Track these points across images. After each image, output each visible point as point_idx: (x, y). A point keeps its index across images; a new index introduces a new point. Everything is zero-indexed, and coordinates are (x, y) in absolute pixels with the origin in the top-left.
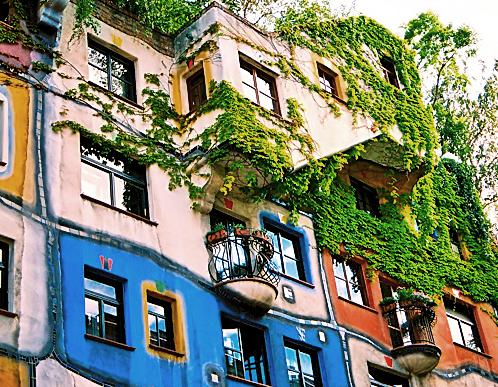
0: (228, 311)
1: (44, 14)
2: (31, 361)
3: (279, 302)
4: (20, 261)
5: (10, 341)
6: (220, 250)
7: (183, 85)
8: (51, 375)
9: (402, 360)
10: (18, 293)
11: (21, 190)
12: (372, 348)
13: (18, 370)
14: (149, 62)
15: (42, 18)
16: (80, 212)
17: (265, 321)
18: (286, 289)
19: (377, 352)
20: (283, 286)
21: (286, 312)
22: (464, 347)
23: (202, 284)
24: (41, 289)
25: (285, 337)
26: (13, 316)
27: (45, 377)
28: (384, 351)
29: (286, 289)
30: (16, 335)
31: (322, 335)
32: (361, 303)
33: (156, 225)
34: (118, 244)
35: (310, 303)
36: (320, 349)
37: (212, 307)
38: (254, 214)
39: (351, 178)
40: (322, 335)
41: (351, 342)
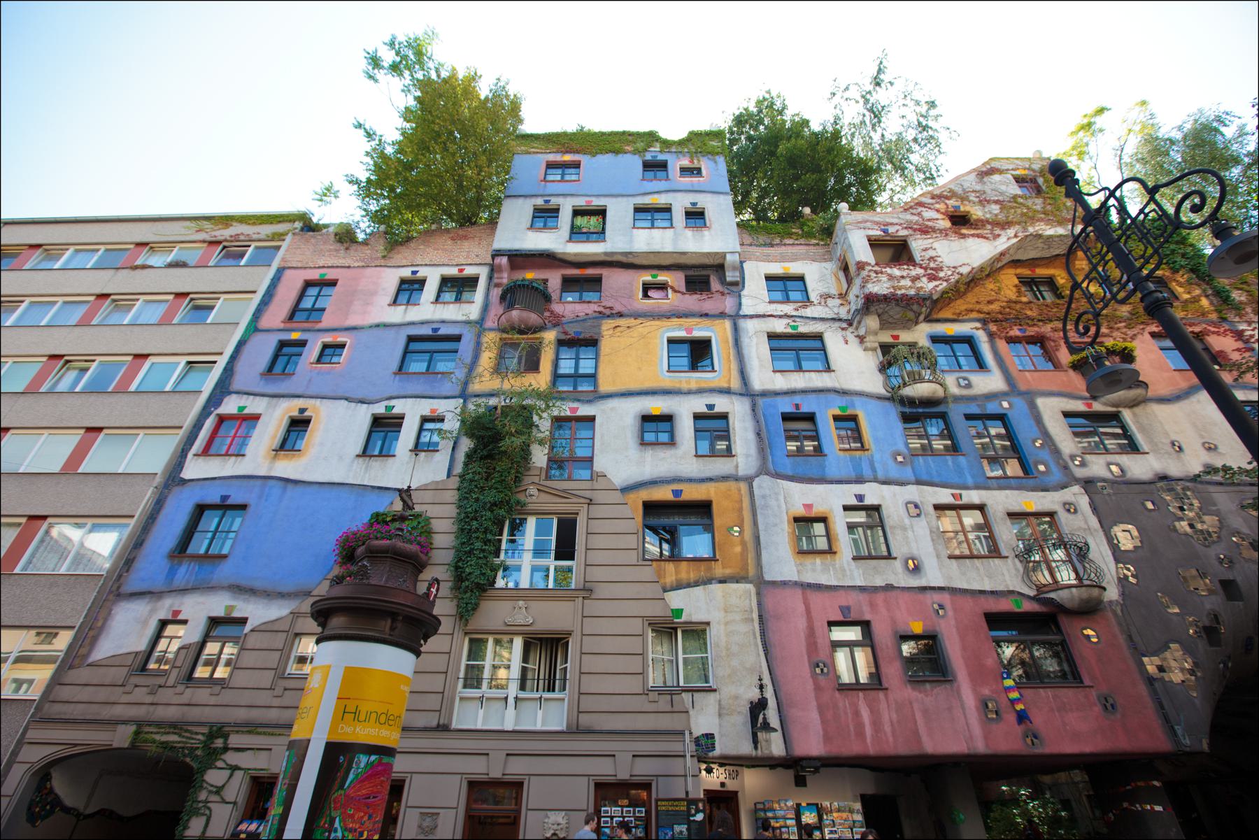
0: (907, 410)
1: (731, 276)
2: (749, 480)
3: (954, 390)
5: (732, 471)
6: (894, 370)
11: (729, 381)
12: (1065, 400)
23: (880, 398)
24: (751, 436)
27: (760, 487)
30: (737, 467)
31: (1005, 404)
34: (804, 392)
35: (991, 382)
37: (892, 413)
40: (1005, 404)
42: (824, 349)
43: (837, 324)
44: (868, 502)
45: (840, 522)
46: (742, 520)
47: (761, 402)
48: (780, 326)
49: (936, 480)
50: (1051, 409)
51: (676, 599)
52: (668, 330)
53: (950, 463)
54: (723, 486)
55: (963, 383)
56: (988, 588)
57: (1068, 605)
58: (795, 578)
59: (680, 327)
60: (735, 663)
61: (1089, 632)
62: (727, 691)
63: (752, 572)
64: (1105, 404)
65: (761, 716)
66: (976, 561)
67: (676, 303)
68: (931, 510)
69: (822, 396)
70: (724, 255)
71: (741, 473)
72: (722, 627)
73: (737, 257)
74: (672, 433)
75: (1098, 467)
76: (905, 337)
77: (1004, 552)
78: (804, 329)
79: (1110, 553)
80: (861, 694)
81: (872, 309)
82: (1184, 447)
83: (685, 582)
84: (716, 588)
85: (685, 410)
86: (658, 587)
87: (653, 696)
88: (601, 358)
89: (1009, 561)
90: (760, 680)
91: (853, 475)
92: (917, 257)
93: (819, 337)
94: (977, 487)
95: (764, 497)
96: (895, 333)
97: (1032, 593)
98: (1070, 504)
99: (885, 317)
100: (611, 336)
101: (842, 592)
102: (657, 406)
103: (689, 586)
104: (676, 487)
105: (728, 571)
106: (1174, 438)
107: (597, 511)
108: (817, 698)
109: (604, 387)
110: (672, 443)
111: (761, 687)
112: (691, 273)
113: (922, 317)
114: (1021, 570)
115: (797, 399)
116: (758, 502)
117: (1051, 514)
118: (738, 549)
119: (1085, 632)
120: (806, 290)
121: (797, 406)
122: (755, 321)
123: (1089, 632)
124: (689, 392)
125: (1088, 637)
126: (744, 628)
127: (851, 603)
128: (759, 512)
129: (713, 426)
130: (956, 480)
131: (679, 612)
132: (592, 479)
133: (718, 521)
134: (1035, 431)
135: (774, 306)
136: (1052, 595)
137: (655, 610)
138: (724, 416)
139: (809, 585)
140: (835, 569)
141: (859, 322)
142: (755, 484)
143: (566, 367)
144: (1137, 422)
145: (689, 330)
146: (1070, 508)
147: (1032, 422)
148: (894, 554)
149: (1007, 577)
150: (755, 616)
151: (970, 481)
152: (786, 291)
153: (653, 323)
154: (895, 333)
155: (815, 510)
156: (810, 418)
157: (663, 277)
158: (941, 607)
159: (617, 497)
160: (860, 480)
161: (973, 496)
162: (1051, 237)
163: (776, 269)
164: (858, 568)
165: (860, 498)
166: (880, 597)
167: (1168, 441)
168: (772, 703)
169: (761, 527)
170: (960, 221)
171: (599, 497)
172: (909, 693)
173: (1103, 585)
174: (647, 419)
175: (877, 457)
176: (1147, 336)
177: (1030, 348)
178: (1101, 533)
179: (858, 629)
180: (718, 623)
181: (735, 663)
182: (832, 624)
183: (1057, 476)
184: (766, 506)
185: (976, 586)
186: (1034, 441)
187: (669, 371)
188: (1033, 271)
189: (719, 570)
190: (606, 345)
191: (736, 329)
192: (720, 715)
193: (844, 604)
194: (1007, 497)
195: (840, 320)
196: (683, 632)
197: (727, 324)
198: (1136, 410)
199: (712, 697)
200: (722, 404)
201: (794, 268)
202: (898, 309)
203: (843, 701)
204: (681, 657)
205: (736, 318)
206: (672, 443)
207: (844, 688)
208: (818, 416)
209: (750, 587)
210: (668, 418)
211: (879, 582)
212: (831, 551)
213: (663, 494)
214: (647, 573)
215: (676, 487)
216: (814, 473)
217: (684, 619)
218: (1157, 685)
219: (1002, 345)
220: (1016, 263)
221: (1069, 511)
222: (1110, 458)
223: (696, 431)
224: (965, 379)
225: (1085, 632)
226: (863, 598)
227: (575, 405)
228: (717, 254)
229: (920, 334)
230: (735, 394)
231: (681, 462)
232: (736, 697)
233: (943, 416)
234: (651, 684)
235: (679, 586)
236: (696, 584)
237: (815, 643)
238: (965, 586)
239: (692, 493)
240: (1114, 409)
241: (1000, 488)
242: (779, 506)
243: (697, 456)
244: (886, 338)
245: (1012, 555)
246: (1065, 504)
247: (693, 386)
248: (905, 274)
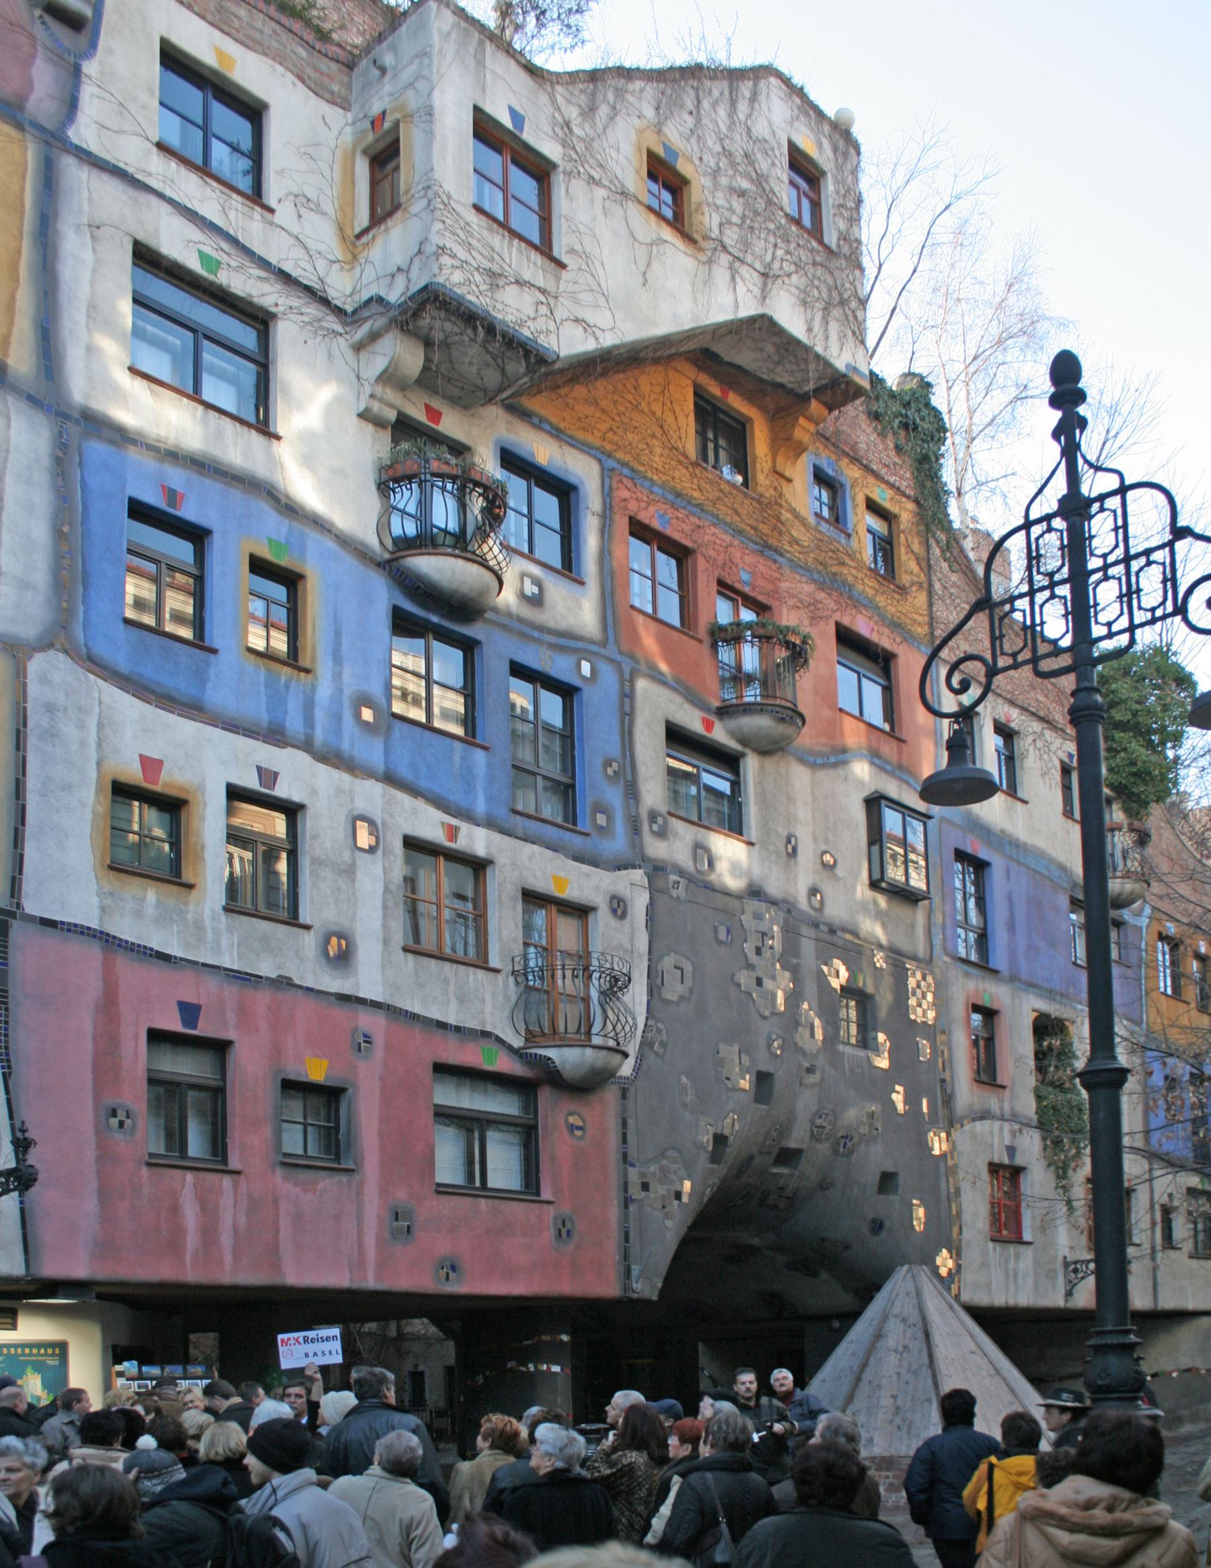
3: (508, 597)
37: (382, 596)
38: (484, 437)
56: (452, 1020)
66: (447, 965)
89: (500, 977)
114: (514, 999)
127: (202, 1001)
149: (488, 1008)
158: (368, 1039)
166: (263, 999)
178: (646, 963)
185: (435, 1013)
226: (231, 991)
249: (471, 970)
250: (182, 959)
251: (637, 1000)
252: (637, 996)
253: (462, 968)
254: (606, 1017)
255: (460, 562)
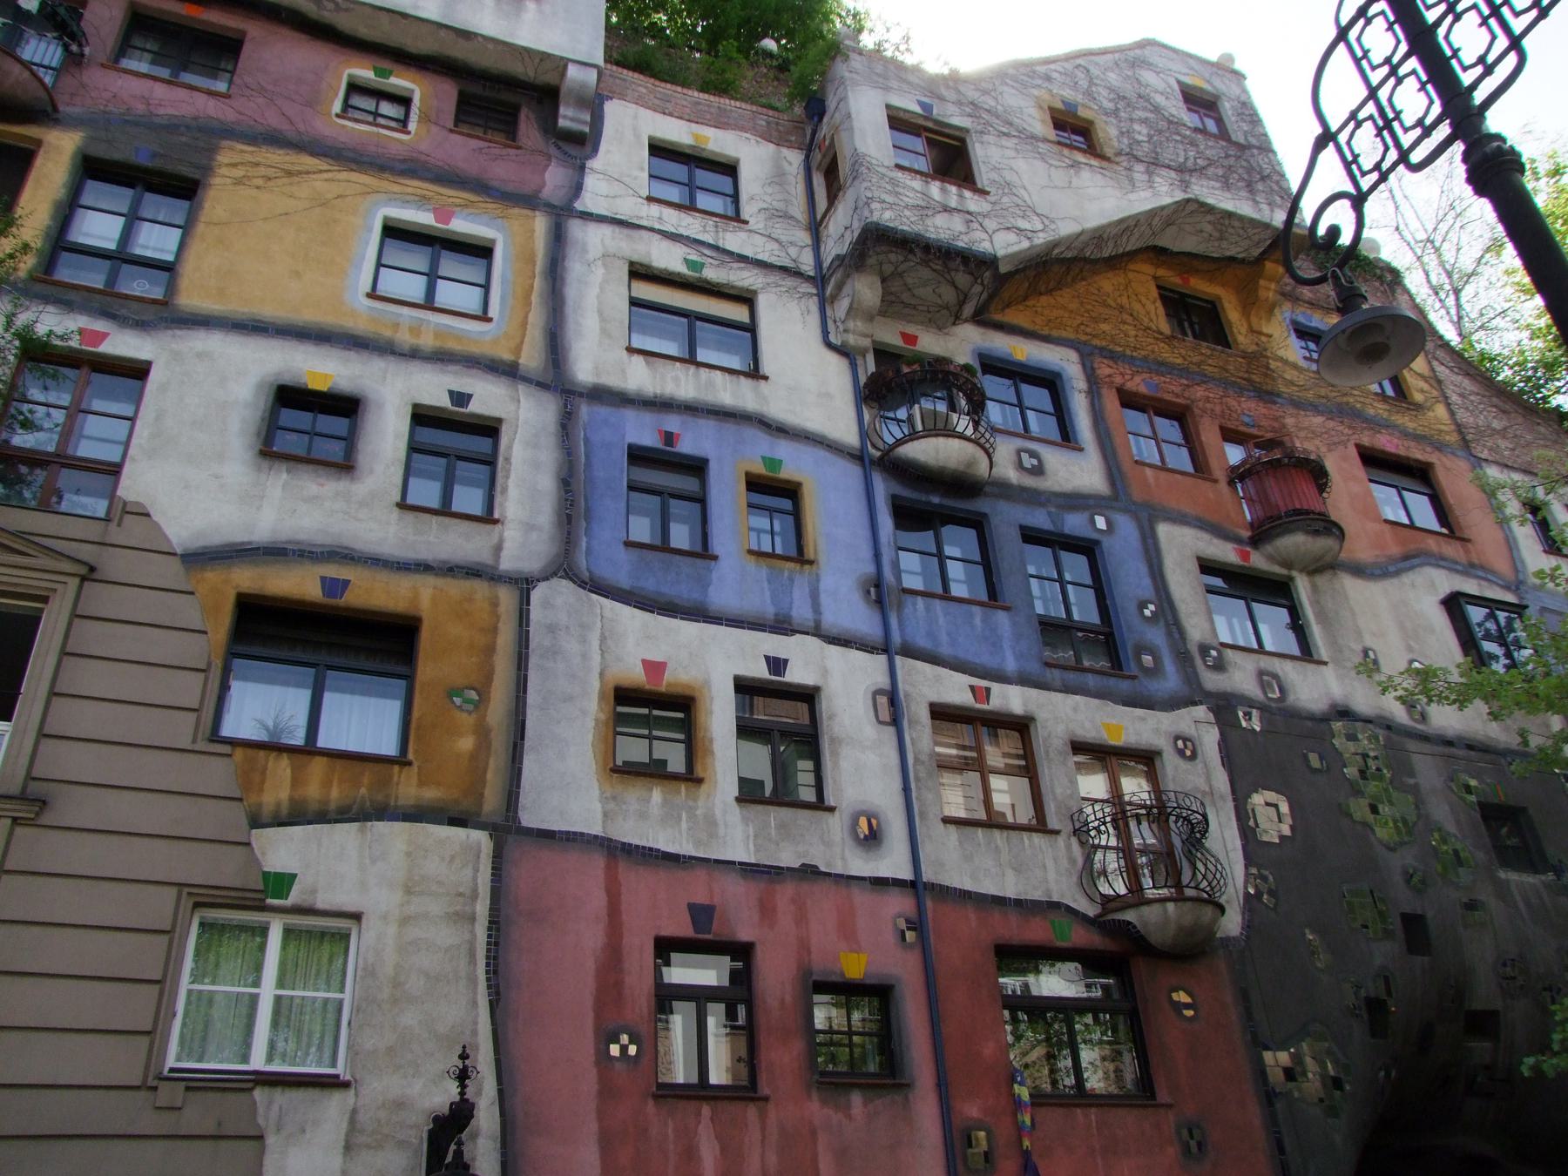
1: (569, 117)
2: (524, 585)
4: (510, 447)
7: (819, 181)
8: (559, 601)
9: (1269, 548)
10: (505, 490)
11: (518, 350)
12: (1206, 536)
13: (497, 597)
14: (763, 163)
15: (562, 123)
16: (623, 371)
17: (980, 505)
18: (1025, 456)
19: (1215, 541)
20: (1019, 452)
21: (1023, 489)
22: (1412, 526)
24: (547, 483)
25: (1022, 528)
26: (496, 522)
27: (547, 604)
28: (1237, 540)
29: (1025, 456)
30: (498, 548)
31: (1101, 522)
32: (1190, 468)
33: (766, 378)
34: (691, 409)
35: (1078, 471)
36: (1097, 542)
39: (1158, 287)
40: (1101, 522)
41: (1163, 530)
42: (751, 329)
43: (790, 282)
44: (796, 675)
45: (720, 717)
46: (489, 677)
47: (585, 410)
48: (669, 258)
49: (945, 650)
50: (1181, 545)
51: (282, 850)
52: (393, 199)
53: (978, 621)
54: (456, 588)
55: (1028, 462)
56: (1011, 892)
57: (1155, 938)
58: (596, 829)
59: (422, 201)
60: (410, 1018)
61: (1182, 997)
62: (378, 1087)
63: (492, 801)
64: (1271, 558)
65: (453, 1147)
66: (997, 833)
67: (424, 147)
68: (924, 715)
69: (730, 428)
70: (561, 64)
71: (507, 564)
72: (392, 930)
73: (592, 76)
74: (350, 441)
75: (1241, 678)
76: (930, 343)
77: (1053, 822)
78: (712, 274)
79: (1238, 843)
80: (706, 1110)
81: (872, 261)
82: (1382, 661)
83: (314, 806)
84: (395, 834)
85: (393, 394)
86: (237, 814)
87: (169, 1094)
88: (200, 228)
89: (1060, 841)
90: (464, 1056)
91: (770, 611)
92: (983, 176)
93: (746, 299)
94: (1024, 680)
95: (552, 629)
96: (911, 329)
97: (1091, 910)
98: (1185, 740)
99: (896, 286)
100: (238, 182)
101: (701, 874)
102: (323, 369)
103: (322, 817)
104: (333, 571)
105: (431, 794)
106: (1369, 641)
107: (101, 599)
108: (601, 1115)
109: (190, 298)
110: (346, 466)
111: (463, 1076)
112: (475, 89)
113: (968, 310)
114: (1080, 861)
115: (673, 423)
116: (537, 637)
117: (1146, 759)
118: (466, 744)
119: (1175, 996)
120: (735, 197)
121: (669, 438)
122: (606, 231)
123: (1182, 997)
124: (414, 354)
125: (1179, 1007)
126: (447, 936)
127: (716, 901)
128: (533, 661)
129: (455, 442)
130: (985, 659)
131: (282, 882)
132: (107, 519)
133: (426, 669)
134: (1145, 587)
135: (655, 209)
136: (1130, 916)
137: (219, 869)
138: (489, 429)
139: (629, 851)
140: (692, 817)
141: (839, 287)
142: (536, 595)
143: (99, 228)
144: (1316, 603)
145: (444, 214)
146: (1188, 749)
147: (1143, 569)
148: (830, 800)
149: (1051, 875)
150: (482, 908)
151: (1011, 665)
152: (691, 187)
153: (354, 176)
154: (911, 329)
155: (668, 677)
156: (697, 467)
157: (400, 81)
159: (171, 573)
160: (782, 626)
161: (1011, 699)
162: (1230, 215)
163: (678, 132)
164: (746, 821)
165: (777, 665)
166: (785, 893)
167: (1359, 648)
168: (486, 1117)
169: (532, 698)
170: (1074, 130)
171: (115, 564)
172: (816, 1109)
173: (1222, 901)
174: (289, 397)
175: (828, 582)
176: (1353, 452)
177: (1158, 421)
178: (1230, 805)
179: (726, 961)
180: (384, 918)
181: (410, 1018)
182: (666, 948)
183: (1171, 681)
184: (554, 652)
185: (989, 887)
186: (1142, 605)
187: (373, 295)
188: (1186, 281)
189: (408, 789)
190: (219, 200)
191: (558, 238)
192: (348, 1148)
193: (701, 898)
194: (1075, 709)
195: (797, 274)
196: (288, 932)
197: (540, 224)
198: (1322, 580)
199: (334, 1106)
200: (488, 397)
201: (719, 142)
202: (925, 273)
203: (662, 1125)
204: (268, 991)
205: (563, 214)
206: (346, 466)
207: (669, 1093)
208: (713, 468)
209: (481, 838)
210: (346, 406)
211: (788, 858)
212: (692, 777)
213: (299, 584)
214: (217, 774)
215: (333, 571)
216: (683, 591)
217: (294, 898)
218: (1279, 1105)
219: (1111, 402)
220: (1158, 254)
221: (1181, 753)
222: (1266, 663)
223: (414, 448)
224: (1033, 454)
225: (1175, 996)
227: (100, 325)
228: (544, 56)
229: (962, 344)
230: (526, 380)
231: (359, 513)
232: (400, 1105)
233: (978, 523)
234: (171, 1062)
235: (297, 815)
236: (343, 815)
237: (619, 984)
238: (968, 885)
239: (373, 593)
240: (1284, 572)
241: (1067, 689)
242: (585, 656)
243: (403, 505)
244: (890, 335)
245: (1067, 828)
246: (1177, 738)
247: (427, 342)
248: (953, 202)
249: (1025, 835)
250: (691, 858)
251: (1230, 847)
252: (1224, 838)
253: (1013, 834)
254: (1195, 868)
255: (941, 440)
